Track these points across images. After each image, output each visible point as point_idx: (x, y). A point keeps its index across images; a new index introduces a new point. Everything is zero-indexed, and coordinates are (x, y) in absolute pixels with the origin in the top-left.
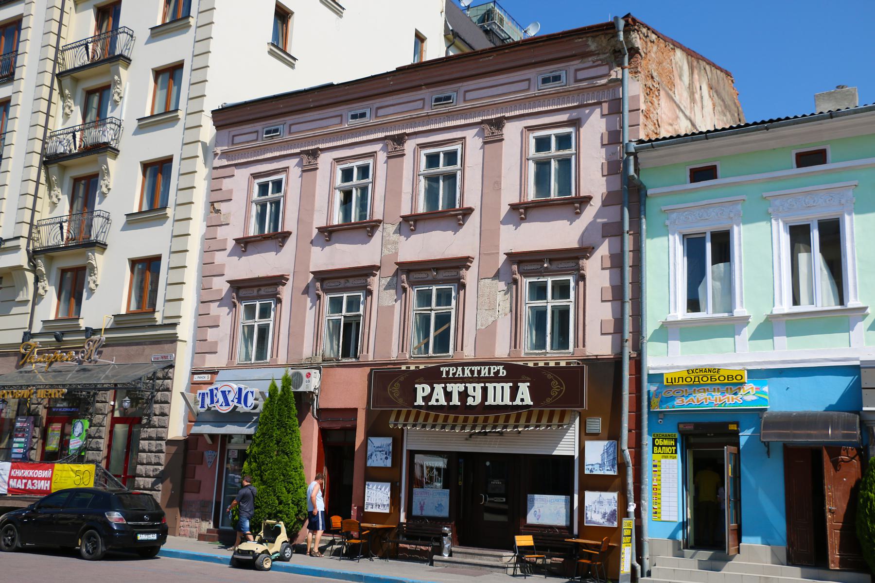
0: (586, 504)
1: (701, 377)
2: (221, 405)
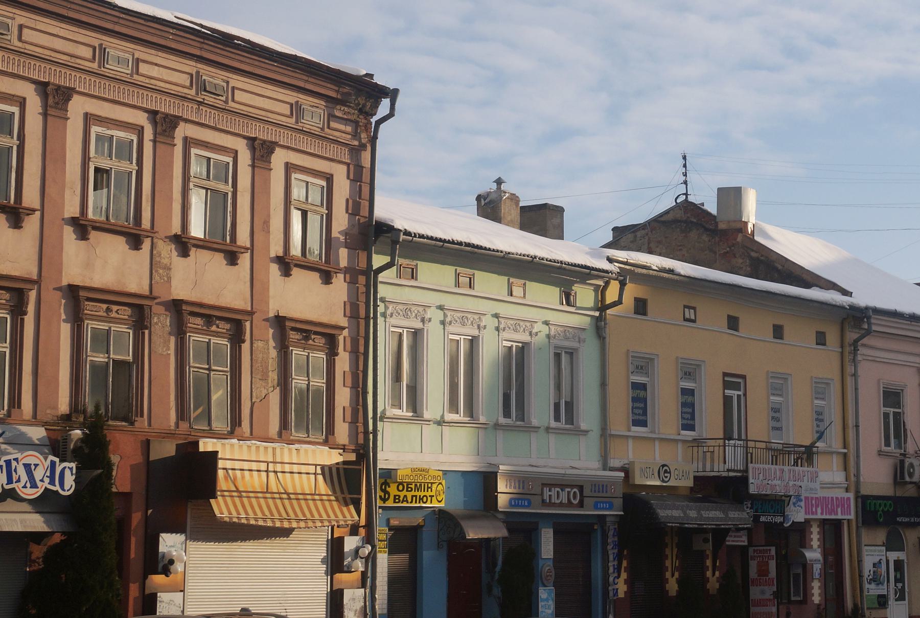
0: (345, 603)
1: (419, 475)
2: (25, 487)
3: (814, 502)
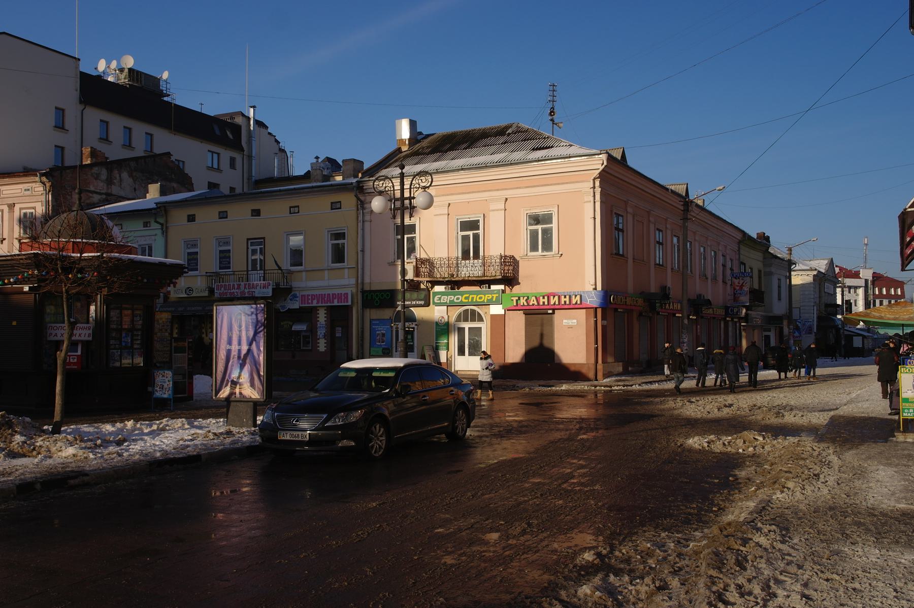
3: (310, 297)
